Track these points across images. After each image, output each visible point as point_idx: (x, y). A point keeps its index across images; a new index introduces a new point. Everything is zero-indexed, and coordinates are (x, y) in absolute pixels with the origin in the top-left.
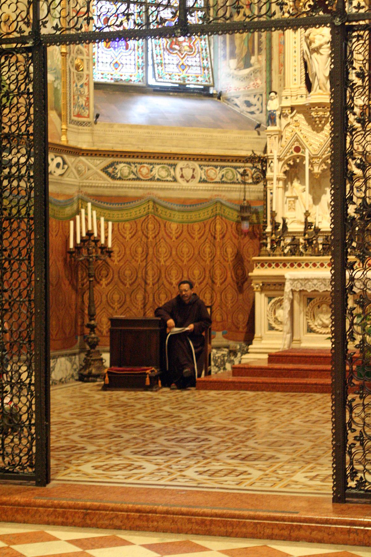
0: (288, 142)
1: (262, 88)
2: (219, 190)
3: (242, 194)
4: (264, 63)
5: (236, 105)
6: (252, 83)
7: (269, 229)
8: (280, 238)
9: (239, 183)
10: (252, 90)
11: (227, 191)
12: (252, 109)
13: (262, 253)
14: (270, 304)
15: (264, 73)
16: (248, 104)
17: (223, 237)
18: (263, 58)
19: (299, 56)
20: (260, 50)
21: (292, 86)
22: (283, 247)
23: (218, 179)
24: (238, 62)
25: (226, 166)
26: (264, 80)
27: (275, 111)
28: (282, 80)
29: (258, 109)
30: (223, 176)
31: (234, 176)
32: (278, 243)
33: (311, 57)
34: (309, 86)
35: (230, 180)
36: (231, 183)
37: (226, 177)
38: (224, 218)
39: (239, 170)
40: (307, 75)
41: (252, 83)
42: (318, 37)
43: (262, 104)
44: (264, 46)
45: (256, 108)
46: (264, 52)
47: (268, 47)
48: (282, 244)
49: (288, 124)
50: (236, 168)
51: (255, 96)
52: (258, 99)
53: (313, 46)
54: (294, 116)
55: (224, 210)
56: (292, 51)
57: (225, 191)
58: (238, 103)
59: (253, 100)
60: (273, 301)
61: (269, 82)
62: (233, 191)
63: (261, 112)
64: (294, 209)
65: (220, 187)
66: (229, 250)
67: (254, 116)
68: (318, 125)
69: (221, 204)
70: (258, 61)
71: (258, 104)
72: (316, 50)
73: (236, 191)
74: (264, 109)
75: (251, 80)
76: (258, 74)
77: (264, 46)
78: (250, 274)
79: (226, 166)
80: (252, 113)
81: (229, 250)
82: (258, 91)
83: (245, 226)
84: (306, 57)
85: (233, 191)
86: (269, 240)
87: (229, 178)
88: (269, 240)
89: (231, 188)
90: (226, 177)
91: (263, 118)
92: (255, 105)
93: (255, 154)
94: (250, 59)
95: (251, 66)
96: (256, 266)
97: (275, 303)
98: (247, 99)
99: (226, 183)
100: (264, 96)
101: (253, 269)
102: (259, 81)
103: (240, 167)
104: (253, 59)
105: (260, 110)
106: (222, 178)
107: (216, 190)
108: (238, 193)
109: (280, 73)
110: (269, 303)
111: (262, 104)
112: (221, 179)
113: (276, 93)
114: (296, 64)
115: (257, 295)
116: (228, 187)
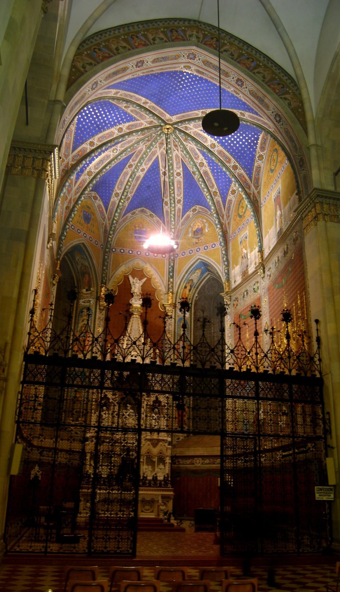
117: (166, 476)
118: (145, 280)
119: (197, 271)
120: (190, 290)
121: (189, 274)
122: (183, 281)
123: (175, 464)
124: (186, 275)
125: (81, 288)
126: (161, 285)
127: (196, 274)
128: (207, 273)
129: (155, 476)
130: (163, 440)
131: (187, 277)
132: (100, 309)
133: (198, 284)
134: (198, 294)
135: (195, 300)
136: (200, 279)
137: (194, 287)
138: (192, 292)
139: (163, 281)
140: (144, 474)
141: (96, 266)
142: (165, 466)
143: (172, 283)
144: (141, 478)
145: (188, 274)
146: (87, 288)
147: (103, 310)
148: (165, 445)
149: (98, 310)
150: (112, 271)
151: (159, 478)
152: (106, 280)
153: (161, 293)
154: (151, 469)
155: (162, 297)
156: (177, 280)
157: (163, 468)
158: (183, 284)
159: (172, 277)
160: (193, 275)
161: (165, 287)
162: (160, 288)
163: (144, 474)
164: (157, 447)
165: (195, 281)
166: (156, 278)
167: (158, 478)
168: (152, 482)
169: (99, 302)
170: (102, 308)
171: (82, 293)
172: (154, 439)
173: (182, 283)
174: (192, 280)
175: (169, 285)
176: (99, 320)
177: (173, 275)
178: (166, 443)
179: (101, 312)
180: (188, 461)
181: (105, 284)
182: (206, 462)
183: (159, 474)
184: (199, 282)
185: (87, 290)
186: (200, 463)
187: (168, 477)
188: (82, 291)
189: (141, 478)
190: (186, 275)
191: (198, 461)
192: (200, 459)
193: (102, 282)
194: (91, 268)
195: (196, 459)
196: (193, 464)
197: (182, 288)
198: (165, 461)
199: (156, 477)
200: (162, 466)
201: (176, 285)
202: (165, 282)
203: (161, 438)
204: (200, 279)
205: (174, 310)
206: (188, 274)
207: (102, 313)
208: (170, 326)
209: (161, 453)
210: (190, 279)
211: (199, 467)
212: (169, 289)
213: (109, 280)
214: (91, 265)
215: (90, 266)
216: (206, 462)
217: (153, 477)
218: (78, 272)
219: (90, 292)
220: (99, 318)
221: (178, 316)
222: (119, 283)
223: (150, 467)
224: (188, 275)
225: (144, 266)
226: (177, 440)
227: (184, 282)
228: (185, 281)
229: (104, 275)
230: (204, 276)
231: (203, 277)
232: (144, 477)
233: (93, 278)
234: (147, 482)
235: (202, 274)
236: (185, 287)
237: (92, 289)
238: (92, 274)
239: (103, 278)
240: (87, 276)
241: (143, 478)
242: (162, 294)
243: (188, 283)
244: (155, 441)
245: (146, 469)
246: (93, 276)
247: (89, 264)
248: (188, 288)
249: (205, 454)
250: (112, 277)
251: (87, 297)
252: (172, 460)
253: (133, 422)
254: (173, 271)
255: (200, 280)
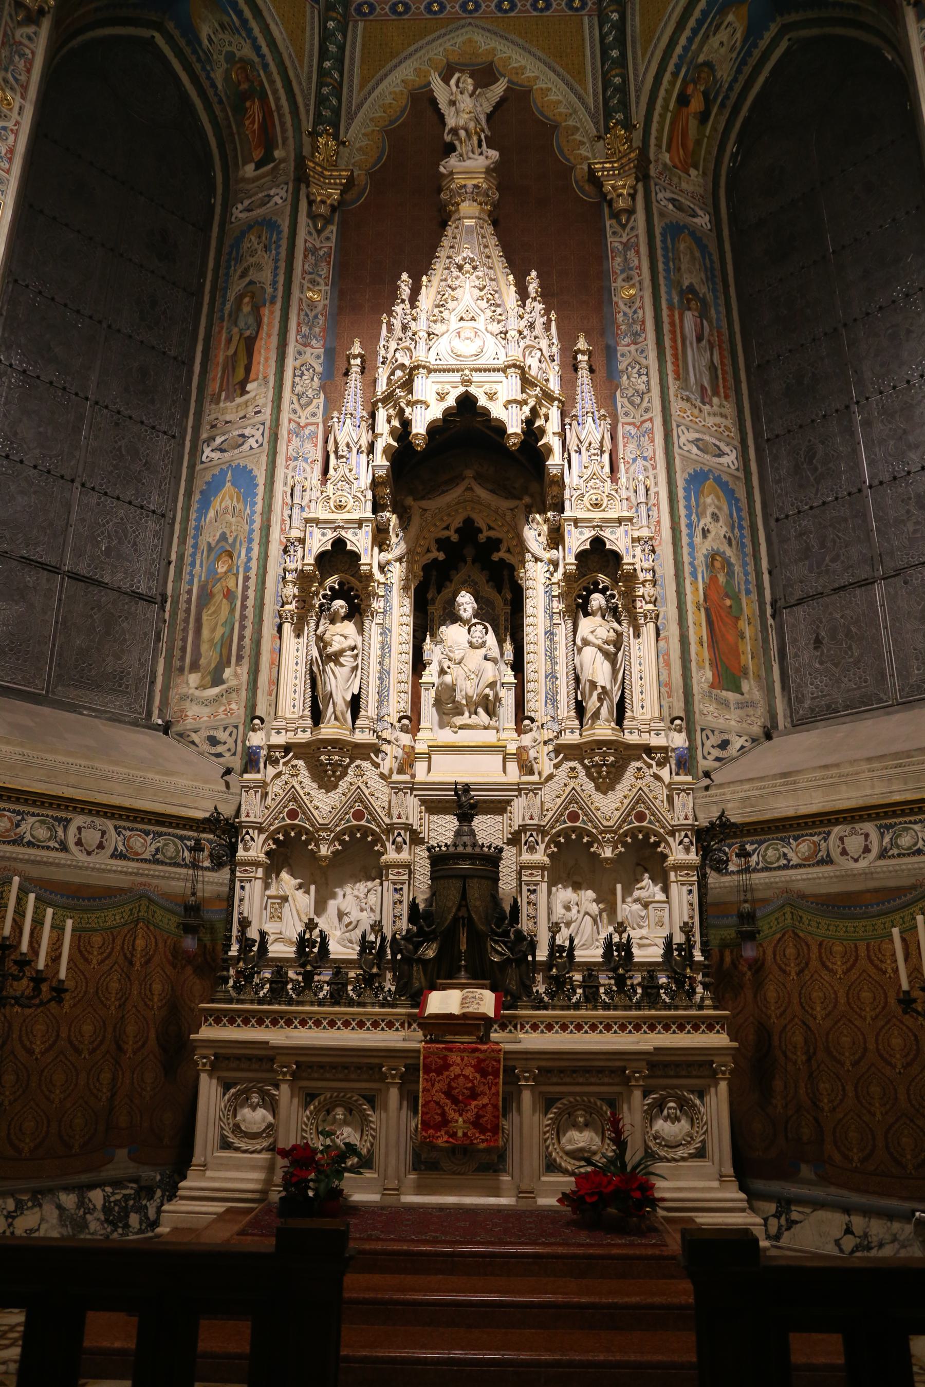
0: (278, 799)
1: (239, 717)
2: (147, 875)
3: (189, 885)
4: (244, 678)
5: (193, 743)
6: (223, 708)
7: (234, 950)
8: (253, 968)
9: (186, 866)
10: (222, 720)
11: (163, 877)
12: (219, 749)
13: (220, 996)
14: (227, 1097)
15: (244, 693)
16: (213, 741)
17: (148, 962)
18: (244, 670)
19: (302, 669)
20: (240, 658)
21: (288, 716)
22: (257, 985)
23: (147, 856)
24: (203, 678)
25: (165, 834)
26: (243, 704)
27: (259, 747)
28: (273, 706)
29: (229, 750)
30: (157, 850)
31: (177, 852)
32: (249, 978)
33: (324, 670)
34: (317, 716)
35: (171, 858)
36: (170, 865)
37: (163, 854)
38: (152, 928)
39: (188, 843)
40: (314, 699)
41: (223, 708)
42: (337, 638)
43: (236, 742)
44: (247, 652)
45: (226, 747)
46: (246, 661)
47: (253, 653)
48: (256, 980)
49: (279, 775)
50: (182, 838)
51: (225, 729)
52: (230, 735)
53: (330, 650)
54: (289, 761)
55: (155, 912)
56: (292, 661)
57: (158, 876)
58: (197, 740)
59: (221, 735)
60: (233, 1091)
61: (251, 706)
62: (173, 878)
63: (234, 754)
64: (280, 918)
65: (149, 870)
66: (157, 987)
67: (221, 760)
68: (330, 777)
69: (150, 900)
70: (236, 675)
71: (230, 741)
72: (335, 658)
73: (178, 879)
74: (239, 748)
75: (222, 704)
76: (234, 695)
77: (247, 652)
78: (193, 1036)
79: (165, 834)
80: (219, 755)
81: (157, 987)
82: (232, 721)
83: (190, 943)
84: (315, 669)
85: (173, 878)
86: (232, 972)
87: (169, 854)
88: (232, 972)
89: (170, 873)
90: (163, 854)
91: (237, 763)
92: (225, 743)
93: (219, 813)
94: (223, 671)
95: (222, 682)
96: (206, 1020)
97: (236, 1096)
98: (212, 733)
99: (163, 863)
100: (241, 728)
101: (200, 1026)
102: (234, 706)
103: (189, 839)
104: (228, 673)
105: (233, 751)
106: (156, 854)
107: (142, 875)
108: (182, 884)
109: (270, 695)
110: (224, 1095)
111: (236, 742)
112: (153, 856)
113: (262, 721)
114: (297, 682)
115: (204, 1077)
116: (165, 872)
117: (679, 938)
118: (498, 89)
119: (730, 18)
120: (703, 117)
121: (695, 32)
122: (671, 67)
123: (720, 867)
124: (683, 41)
125: (236, 165)
126: (575, 112)
127: (723, 35)
128: (774, 28)
129: (616, 939)
130: (649, 750)
131: (686, 49)
132: (312, 216)
133: (738, 87)
134: (740, 140)
135: (730, 170)
136: (744, 62)
137: (723, 105)
138: (714, 129)
139: (580, 98)
140: (555, 929)
141: (282, 48)
142: (666, 890)
143: (623, 90)
144: (542, 955)
145: (687, 33)
146: (258, 155)
147: (328, 221)
148: (657, 777)
149: (303, 218)
150: (362, 86)
151: (639, 955)
152: (337, 112)
153: (578, 137)
154: (594, 908)
155: (584, 152)
156: (642, 70)
157: (661, 896)
158: (672, 83)
159: (622, 62)
160: (714, 41)
161: (592, 117)
162: (570, 123)
163: (555, 929)
164: (618, 787)
165: (724, 73)
166: (549, 90)
167: (635, 951)
168: (603, 979)
169: (308, 186)
170: (323, 210)
171: (244, 180)
172: (600, 743)
173: (667, 77)
174: (708, 64)
175: (606, 101)
176: (311, 259)
177: (623, 55)
178: (660, 764)
179: (319, 232)
180: (798, 850)
181: (336, 126)
182: (905, 841)
183: (644, 932)
184: (742, 79)
185: (258, 166)
186: (867, 850)
187: (688, 946)
188: (241, 173)
189: (542, 955)
190: (683, 41)
191: (854, 844)
192: (869, 827)
193: (319, 119)
194: (265, 66)
195: (837, 830)
196: (828, 861)
197: (665, 108)
198: (665, 857)
199: (627, 947)
200: (649, 889)
201: (638, 91)
202: (590, 101)
203: (632, 738)
204: (744, 62)
205: (640, 186)
206: (687, 33)
207: (326, 233)
208: (631, 254)
209: (641, 817)
210: (701, 59)
211: (867, 874)
212: (608, 116)
213: (351, 118)
214: (265, 50)
215: (262, 57)
216: (905, 841)
217: (609, 945)
218: (220, 102)
219: (272, 165)
220: (310, 251)
221: (662, 214)
222: (396, 121)
223: (590, 894)
224: (690, 40)
225: (494, 49)
226: (716, 753)
227: (675, 75)
228: (678, 67)
229: (325, 90)
230: (763, 44)
231: (757, 53)
232: (554, 948)
233: (279, 108)
234: (578, 977)
235: (753, 32)
236: (683, 100)
237: (277, 154)
238: (275, 92)
239: (321, 100)
240: (254, 108)
241: (551, 955)
242: (583, 143)
243: (695, 82)
244: (604, 755)
245: (568, 908)
246: (277, 100)
247: (257, 49)
248: (696, 104)
249: (897, 798)
250: (360, 106)
251: (261, 188)
252: (705, 852)
253: (490, 672)
254: (621, 42)
255: (747, 70)
